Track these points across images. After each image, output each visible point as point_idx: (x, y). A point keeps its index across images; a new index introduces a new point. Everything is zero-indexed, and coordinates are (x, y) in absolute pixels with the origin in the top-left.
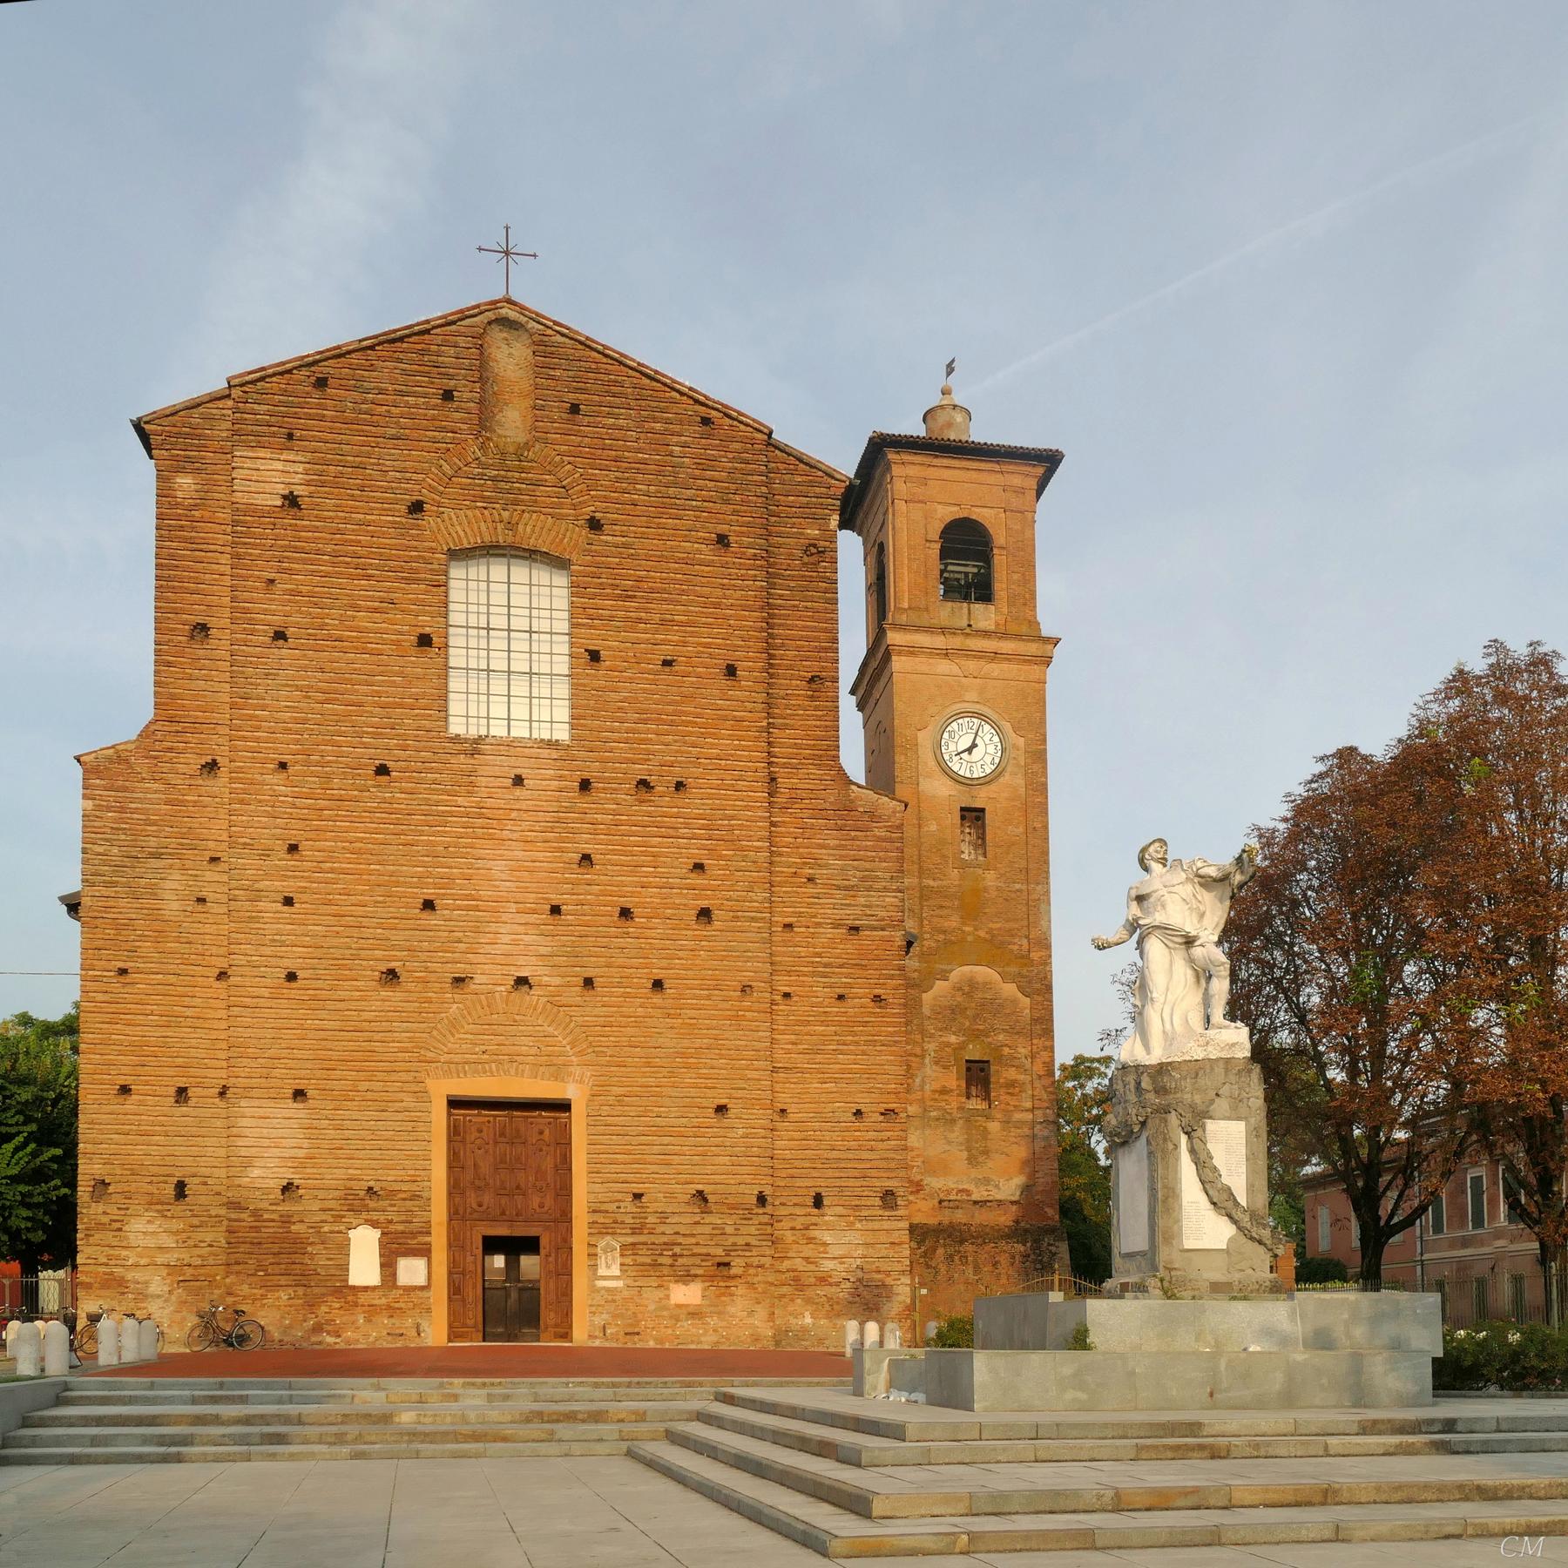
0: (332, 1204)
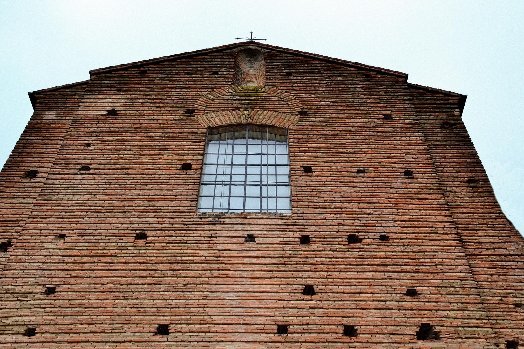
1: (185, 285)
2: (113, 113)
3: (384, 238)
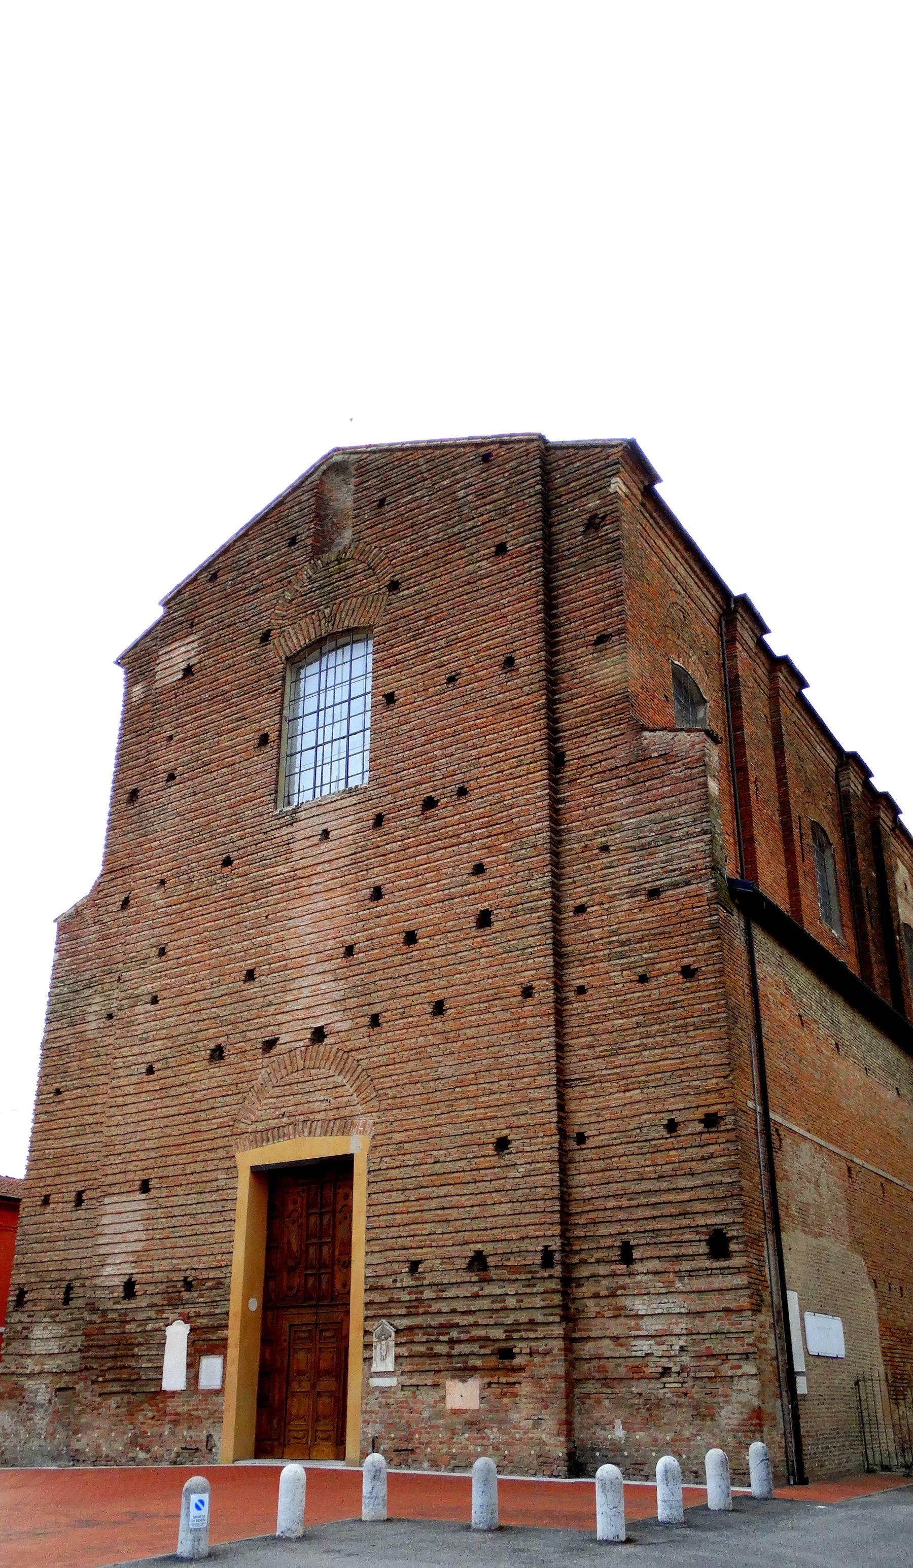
0: (157, 1300)
1: (266, 917)
2: (188, 671)
3: (462, 792)
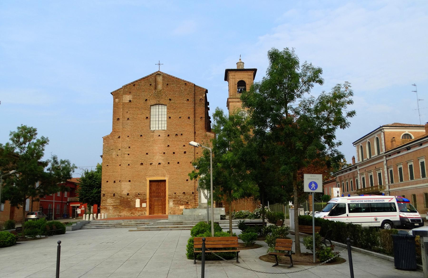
2: (130, 101)
3: (182, 135)
